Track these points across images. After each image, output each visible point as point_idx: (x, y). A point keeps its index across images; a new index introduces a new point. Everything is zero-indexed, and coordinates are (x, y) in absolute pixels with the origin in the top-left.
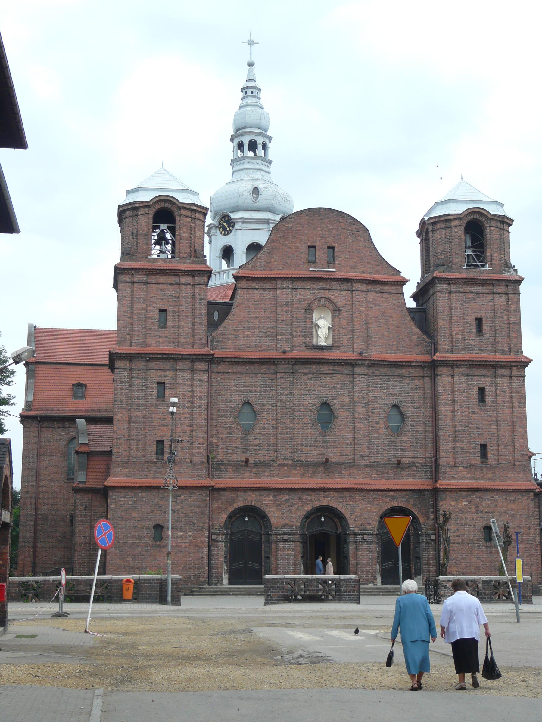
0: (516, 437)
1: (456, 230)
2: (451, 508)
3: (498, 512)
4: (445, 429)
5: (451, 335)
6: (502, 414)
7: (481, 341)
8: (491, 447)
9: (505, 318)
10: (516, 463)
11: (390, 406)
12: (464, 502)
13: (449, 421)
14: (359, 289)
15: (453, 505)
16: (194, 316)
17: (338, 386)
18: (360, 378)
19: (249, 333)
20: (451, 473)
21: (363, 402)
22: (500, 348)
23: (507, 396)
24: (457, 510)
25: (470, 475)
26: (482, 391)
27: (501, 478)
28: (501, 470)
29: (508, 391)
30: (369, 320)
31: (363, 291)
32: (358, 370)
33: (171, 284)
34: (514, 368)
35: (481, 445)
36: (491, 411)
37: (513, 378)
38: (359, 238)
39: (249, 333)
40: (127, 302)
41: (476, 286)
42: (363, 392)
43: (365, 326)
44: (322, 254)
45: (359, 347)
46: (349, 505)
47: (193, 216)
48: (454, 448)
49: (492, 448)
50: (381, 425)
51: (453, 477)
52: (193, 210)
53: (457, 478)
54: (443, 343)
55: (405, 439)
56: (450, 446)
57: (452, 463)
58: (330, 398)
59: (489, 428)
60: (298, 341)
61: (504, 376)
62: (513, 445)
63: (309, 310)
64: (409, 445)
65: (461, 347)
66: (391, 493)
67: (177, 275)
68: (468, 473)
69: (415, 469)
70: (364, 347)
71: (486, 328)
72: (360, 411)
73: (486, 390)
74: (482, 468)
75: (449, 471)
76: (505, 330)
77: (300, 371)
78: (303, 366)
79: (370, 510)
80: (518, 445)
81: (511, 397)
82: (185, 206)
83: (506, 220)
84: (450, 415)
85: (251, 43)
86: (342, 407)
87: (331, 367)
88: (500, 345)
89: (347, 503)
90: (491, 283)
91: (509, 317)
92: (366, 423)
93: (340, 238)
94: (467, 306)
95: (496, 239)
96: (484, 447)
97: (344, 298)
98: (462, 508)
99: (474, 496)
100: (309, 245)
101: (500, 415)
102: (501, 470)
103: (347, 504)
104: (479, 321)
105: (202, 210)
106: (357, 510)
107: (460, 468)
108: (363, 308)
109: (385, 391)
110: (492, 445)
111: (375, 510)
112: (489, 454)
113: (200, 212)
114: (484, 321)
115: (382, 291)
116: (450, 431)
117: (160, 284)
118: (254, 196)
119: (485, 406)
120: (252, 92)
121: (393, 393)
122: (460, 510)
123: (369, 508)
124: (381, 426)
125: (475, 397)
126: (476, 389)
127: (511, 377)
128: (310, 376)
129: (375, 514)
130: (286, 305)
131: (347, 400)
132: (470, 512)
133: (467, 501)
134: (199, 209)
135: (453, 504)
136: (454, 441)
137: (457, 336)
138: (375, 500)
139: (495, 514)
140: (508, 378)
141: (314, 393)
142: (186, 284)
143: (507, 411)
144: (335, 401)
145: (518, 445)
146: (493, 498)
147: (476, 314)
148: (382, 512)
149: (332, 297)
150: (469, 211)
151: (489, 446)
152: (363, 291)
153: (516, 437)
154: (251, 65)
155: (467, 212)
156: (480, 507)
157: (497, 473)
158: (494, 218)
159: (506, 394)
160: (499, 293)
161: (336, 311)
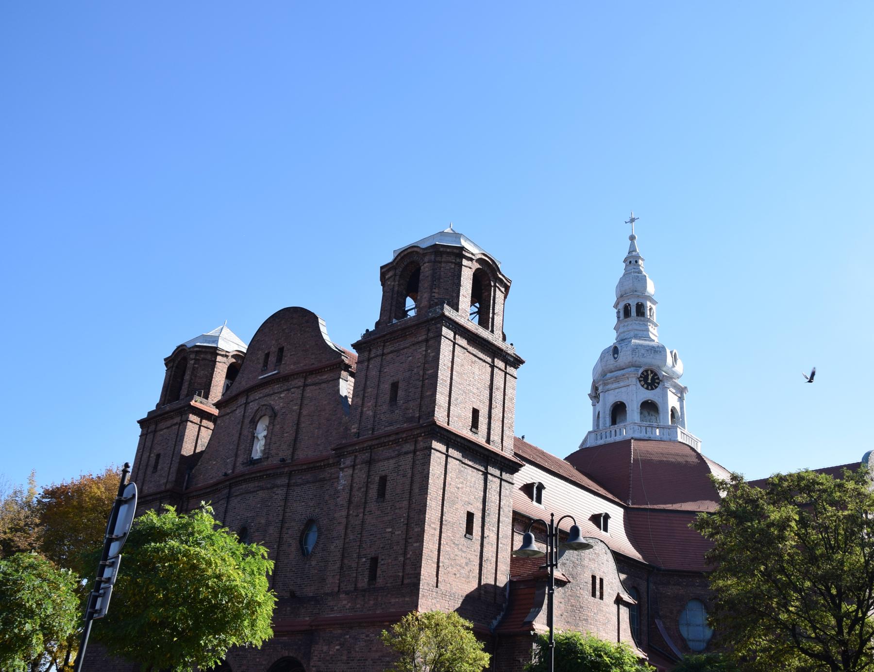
0: (410, 541)
1: (389, 283)
2: (322, 655)
3: (372, 660)
4: (337, 541)
5: (362, 413)
6: (400, 508)
7: (393, 412)
8: (382, 560)
9: (421, 373)
10: (406, 581)
11: (305, 522)
12: (337, 645)
13: (341, 529)
14: (296, 386)
15: (324, 651)
16: (173, 455)
17: (259, 505)
18: (279, 492)
19: (214, 463)
20: (331, 604)
21: (277, 521)
22: (411, 415)
23: (408, 481)
24: (328, 658)
25: (350, 604)
26: (383, 480)
27: (383, 606)
28: (385, 593)
29: (409, 475)
30: (302, 419)
31: (298, 387)
32: (279, 482)
33: (168, 428)
34: (420, 439)
35: (372, 558)
36: (389, 508)
37: (418, 453)
38: (307, 329)
39: (214, 463)
40: (139, 454)
41: (398, 342)
42: (279, 508)
43: (295, 427)
44: (273, 359)
45: (285, 452)
46: (239, 655)
47: (197, 358)
48: (341, 568)
49: (382, 562)
50: (293, 549)
51: (332, 609)
52: (197, 352)
53: (336, 610)
54: (353, 426)
55: (314, 563)
56: (338, 565)
57: (336, 589)
58: (249, 521)
59: (384, 533)
60: (240, 460)
61: (406, 453)
62: (405, 553)
63: (254, 423)
64: (316, 571)
65: (369, 426)
66: (284, 638)
67: (172, 418)
68: (348, 602)
69: (313, 603)
70: (290, 452)
71: (401, 393)
72: (272, 532)
73: (388, 478)
74: (364, 593)
75: (329, 601)
76: (420, 389)
77: (235, 494)
78: (237, 488)
79: (259, 662)
80: (411, 553)
81: (412, 482)
82: (191, 350)
83: (441, 249)
84: (344, 520)
85: (632, 220)
86: (257, 530)
87: (256, 484)
88: (411, 411)
89: (237, 653)
90: (410, 332)
91: (424, 370)
92: (275, 546)
93: (291, 335)
94: (385, 370)
95: (428, 277)
96: (374, 561)
97: (282, 401)
98: (334, 655)
99: (348, 636)
100: (266, 352)
101: (397, 511)
102: (385, 593)
103: (236, 655)
104: (395, 386)
105: (207, 350)
106: (245, 662)
107: (342, 596)
108: (296, 407)
109: (303, 504)
110: (383, 557)
111: (264, 663)
112: (379, 572)
113: (206, 353)
114: (400, 385)
115: (320, 381)
116: (339, 543)
117: (162, 430)
118: (616, 356)
119: (383, 502)
120: (630, 262)
121: (312, 505)
122: (331, 658)
123: (258, 660)
124: (293, 549)
125: (373, 492)
126: (377, 479)
127: (415, 452)
128: (239, 498)
129: (263, 667)
130: (238, 423)
131: (263, 521)
132: (341, 660)
133: (340, 644)
134: (204, 350)
135: (325, 648)
136: (343, 556)
137: (368, 412)
138: (266, 648)
139: (367, 663)
140: (411, 455)
141: (239, 517)
142: (175, 425)
143: (405, 503)
144: (252, 524)
145: (411, 553)
146: (368, 638)
147: (394, 378)
148: (270, 664)
149: (272, 403)
150: (402, 255)
151: (379, 560)
152: (298, 387)
153: (410, 541)
154: (632, 238)
155: (399, 257)
156: (353, 652)
157: (379, 599)
158: (426, 252)
159: (407, 478)
160: (418, 343)
161: (274, 416)
